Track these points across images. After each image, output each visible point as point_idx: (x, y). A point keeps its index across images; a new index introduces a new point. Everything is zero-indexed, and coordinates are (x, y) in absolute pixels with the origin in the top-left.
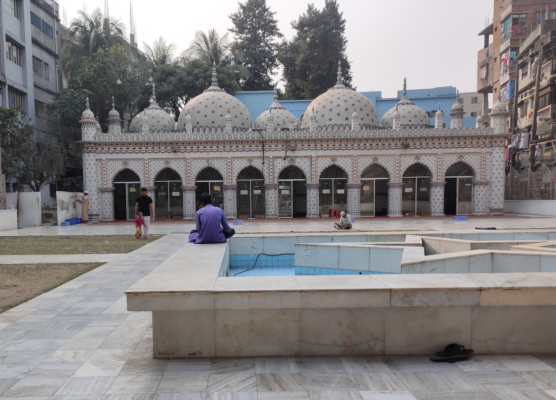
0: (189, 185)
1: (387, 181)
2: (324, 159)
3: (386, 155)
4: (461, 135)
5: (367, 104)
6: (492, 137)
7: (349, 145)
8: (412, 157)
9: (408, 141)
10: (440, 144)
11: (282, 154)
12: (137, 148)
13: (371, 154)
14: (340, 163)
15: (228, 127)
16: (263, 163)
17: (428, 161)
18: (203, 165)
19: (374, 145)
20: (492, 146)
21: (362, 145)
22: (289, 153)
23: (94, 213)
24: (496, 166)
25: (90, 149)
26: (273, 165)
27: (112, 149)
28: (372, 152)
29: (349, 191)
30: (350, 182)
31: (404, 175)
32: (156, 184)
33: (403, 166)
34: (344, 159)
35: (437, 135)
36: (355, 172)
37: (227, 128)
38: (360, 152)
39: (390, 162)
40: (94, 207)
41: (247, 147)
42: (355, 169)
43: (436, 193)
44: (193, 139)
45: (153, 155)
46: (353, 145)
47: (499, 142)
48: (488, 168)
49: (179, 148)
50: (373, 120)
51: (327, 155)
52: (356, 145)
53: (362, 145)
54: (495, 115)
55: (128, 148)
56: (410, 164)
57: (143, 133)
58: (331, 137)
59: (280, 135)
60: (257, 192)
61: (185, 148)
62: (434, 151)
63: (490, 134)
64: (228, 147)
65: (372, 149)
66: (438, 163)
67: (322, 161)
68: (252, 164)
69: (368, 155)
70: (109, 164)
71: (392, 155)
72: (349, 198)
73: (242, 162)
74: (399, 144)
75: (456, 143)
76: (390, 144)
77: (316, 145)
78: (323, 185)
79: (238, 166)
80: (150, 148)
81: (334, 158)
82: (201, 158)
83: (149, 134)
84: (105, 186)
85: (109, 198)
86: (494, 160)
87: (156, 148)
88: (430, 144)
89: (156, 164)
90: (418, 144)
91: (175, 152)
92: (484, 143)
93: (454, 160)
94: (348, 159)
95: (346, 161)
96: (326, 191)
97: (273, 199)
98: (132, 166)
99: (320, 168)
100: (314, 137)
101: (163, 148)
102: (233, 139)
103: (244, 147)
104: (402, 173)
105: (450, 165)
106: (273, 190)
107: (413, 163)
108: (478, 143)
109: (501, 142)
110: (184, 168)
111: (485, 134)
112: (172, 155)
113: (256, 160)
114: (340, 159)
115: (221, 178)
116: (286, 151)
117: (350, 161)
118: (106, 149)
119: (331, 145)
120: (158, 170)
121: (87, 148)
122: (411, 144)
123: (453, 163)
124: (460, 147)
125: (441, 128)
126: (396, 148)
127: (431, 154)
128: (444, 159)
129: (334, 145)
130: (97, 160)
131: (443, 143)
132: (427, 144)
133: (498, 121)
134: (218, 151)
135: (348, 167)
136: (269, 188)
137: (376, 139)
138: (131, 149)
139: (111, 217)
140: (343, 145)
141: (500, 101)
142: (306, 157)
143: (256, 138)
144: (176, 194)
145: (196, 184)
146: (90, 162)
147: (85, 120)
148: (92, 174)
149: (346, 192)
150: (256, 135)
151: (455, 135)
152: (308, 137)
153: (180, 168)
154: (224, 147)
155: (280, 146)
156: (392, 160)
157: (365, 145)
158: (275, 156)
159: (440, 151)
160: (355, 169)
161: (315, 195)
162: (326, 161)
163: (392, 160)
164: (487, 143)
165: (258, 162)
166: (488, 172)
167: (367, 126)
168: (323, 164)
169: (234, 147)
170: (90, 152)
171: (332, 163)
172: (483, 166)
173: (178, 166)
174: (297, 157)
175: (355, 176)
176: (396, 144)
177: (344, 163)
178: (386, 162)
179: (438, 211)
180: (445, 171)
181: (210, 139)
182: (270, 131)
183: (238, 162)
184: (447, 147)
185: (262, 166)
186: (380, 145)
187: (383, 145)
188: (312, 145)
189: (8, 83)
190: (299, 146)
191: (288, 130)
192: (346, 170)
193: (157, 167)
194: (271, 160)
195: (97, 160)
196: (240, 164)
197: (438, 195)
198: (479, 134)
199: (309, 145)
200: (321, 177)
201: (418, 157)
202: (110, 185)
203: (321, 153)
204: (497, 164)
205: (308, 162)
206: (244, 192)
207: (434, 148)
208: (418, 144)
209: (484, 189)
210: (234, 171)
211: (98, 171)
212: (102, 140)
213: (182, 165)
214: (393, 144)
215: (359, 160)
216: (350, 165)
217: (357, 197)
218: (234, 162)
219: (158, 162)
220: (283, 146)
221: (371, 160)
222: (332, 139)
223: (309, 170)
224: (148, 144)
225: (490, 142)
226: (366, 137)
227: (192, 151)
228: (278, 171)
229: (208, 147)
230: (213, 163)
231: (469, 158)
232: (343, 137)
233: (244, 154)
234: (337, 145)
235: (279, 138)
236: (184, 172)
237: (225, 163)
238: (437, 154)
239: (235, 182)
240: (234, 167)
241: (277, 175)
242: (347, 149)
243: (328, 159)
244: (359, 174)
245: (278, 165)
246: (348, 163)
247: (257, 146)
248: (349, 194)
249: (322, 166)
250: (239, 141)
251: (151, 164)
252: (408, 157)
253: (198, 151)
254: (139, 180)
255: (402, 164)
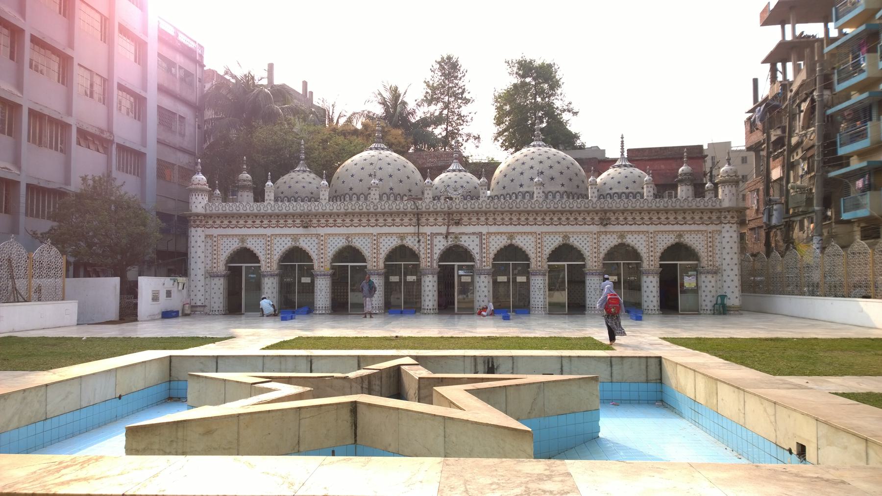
0: (322, 269)
1: (584, 266)
2: (498, 237)
3: (580, 232)
4: (678, 207)
5: (570, 166)
6: (720, 211)
7: (531, 219)
8: (615, 236)
9: (608, 214)
10: (650, 219)
11: (443, 230)
12: (258, 222)
13: (560, 230)
14: (519, 242)
15: (374, 195)
16: (419, 241)
17: (638, 242)
18: (341, 243)
19: (564, 219)
20: (721, 223)
21: (547, 219)
22: (454, 229)
23: (199, 304)
24: (728, 249)
25: (198, 223)
26: (432, 244)
27: (226, 222)
28: (561, 228)
29: (532, 277)
30: (533, 266)
31: (604, 259)
32: (281, 267)
33: (603, 247)
34: (525, 237)
35: (646, 207)
36: (539, 254)
37: (372, 196)
38: (544, 229)
39: (585, 242)
40: (199, 296)
41: (398, 220)
42: (539, 250)
43: (648, 283)
44: (328, 210)
45: (277, 231)
46: (535, 219)
47: (729, 217)
48: (717, 251)
49: (311, 221)
50: (578, 186)
51: (502, 231)
52: (539, 219)
53: (547, 219)
54: (723, 182)
55: (246, 222)
56: (612, 245)
57: (265, 203)
58: (507, 209)
59: (441, 205)
60: (410, 278)
61: (319, 221)
62: (644, 228)
63: (718, 206)
64: (373, 220)
65: (560, 224)
66: (649, 242)
67: (496, 239)
68: (405, 242)
69: (556, 233)
70: (221, 242)
71: (588, 233)
72: (532, 289)
73: (392, 240)
74: (597, 218)
75: (672, 218)
76: (584, 219)
77: (487, 219)
78: (497, 270)
79: (386, 245)
80: (274, 222)
81: (511, 236)
82: (339, 235)
83: (272, 203)
84: (215, 270)
85: (219, 285)
86: (725, 241)
87: (282, 221)
88: (638, 218)
89: (281, 241)
90: (621, 218)
91: (307, 227)
92: (710, 218)
93: (670, 240)
94: (530, 237)
95: (527, 239)
96: (502, 279)
97: (430, 288)
98: (251, 244)
99: (493, 248)
100: (484, 208)
101: (290, 221)
102: (379, 210)
103: (394, 220)
104: (602, 256)
105: (665, 246)
106: (430, 276)
107: (617, 243)
108: (701, 218)
109: (733, 217)
110: (316, 246)
111: (710, 207)
112: (301, 231)
113: (410, 237)
114: (519, 237)
115: (364, 261)
116: (448, 226)
117: (533, 239)
118: (218, 222)
119: (507, 219)
120: (283, 249)
121: (195, 222)
122: (613, 218)
123: (669, 243)
124: (677, 223)
125: (650, 199)
126: (593, 224)
127: (639, 232)
128: (657, 238)
129: (511, 219)
130: (207, 236)
131: (655, 218)
132: (634, 219)
133: (727, 189)
134: (360, 225)
135: (530, 248)
136: (425, 274)
137: (565, 211)
138: (250, 222)
139: (221, 308)
140: (523, 219)
141: (729, 164)
142: (474, 234)
143: (409, 209)
144: (306, 280)
145: (333, 267)
146: (198, 237)
147: (194, 186)
148: (199, 253)
149: (528, 279)
150: (410, 206)
151: (670, 207)
152: (476, 209)
153: (311, 246)
154: (369, 220)
155: (440, 219)
156: (588, 239)
157: (551, 219)
158: (434, 232)
159: (652, 228)
160: (539, 250)
161: (486, 284)
162: (501, 239)
163: (588, 239)
164: (714, 218)
165: (412, 240)
166: (717, 256)
167: (569, 195)
168: (497, 243)
169: (381, 220)
170: (198, 226)
171: (509, 242)
172: (710, 249)
173: (309, 244)
174: (463, 234)
175: (539, 259)
176: (593, 219)
177: (524, 242)
178: (580, 241)
179: (651, 307)
180: (659, 254)
181: (350, 210)
182: (427, 201)
183: (386, 240)
184: (660, 223)
185: (417, 245)
186: (572, 219)
187: (576, 219)
188: (483, 219)
189: (116, 140)
190: (465, 219)
191: (451, 199)
192: (528, 252)
193: (282, 246)
194: (429, 238)
195: (207, 236)
196: (389, 243)
197: (651, 286)
198: (702, 207)
199: (478, 219)
200: (494, 259)
201: (622, 235)
202: (221, 268)
203: (493, 229)
204: (728, 246)
205: (477, 241)
206: (394, 279)
207: (643, 224)
208: (621, 218)
209: (713, 280)
210: (381, 251)
211: (207, 249)
212: (214, 211)
213: (314, 244)
214: (588, 219)
215: (545, 239)
216: (533, 245)
217: (542, 286)
218: (381, 240)
219: (283, 239)
220: (444, 219)
221: (561, 239)
222: (507, 211)
223: (478, 251)
224: (271, 216)
225: (719, 218)
226: (552, 208)
227: (327, 226)
228: (438, 250)
229: (348, 220)
230: (354, 240)
231: (691, 238)
232: (522, 208)
233: (394, 230)
234: (515, 219)
235: (439, 209)
236: (316, 252)
237: (369, 240)
238: (647, 232)
239: (381, 265)
240: (381, 246)
241: (436, 257)
242: (527, 224)
243: (504, 237)
244: (545, 257)
245: (438, 244)
246: (530, 242)
247: (410, 220)
248: (532, 282)
249: (496, 245)
250: (387, 213)
251: (275, 241)
252: (609, 236)
253: (335, 226)
254: (259, 262)
255: (601, 244)
